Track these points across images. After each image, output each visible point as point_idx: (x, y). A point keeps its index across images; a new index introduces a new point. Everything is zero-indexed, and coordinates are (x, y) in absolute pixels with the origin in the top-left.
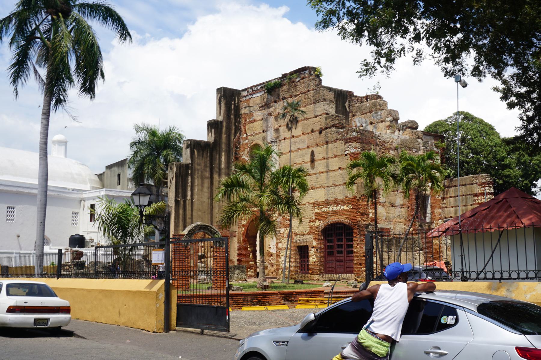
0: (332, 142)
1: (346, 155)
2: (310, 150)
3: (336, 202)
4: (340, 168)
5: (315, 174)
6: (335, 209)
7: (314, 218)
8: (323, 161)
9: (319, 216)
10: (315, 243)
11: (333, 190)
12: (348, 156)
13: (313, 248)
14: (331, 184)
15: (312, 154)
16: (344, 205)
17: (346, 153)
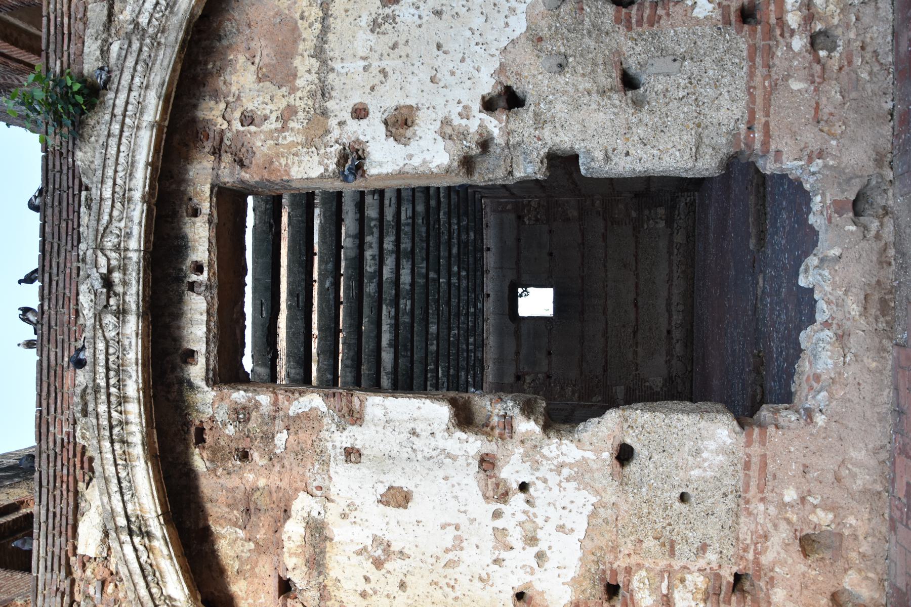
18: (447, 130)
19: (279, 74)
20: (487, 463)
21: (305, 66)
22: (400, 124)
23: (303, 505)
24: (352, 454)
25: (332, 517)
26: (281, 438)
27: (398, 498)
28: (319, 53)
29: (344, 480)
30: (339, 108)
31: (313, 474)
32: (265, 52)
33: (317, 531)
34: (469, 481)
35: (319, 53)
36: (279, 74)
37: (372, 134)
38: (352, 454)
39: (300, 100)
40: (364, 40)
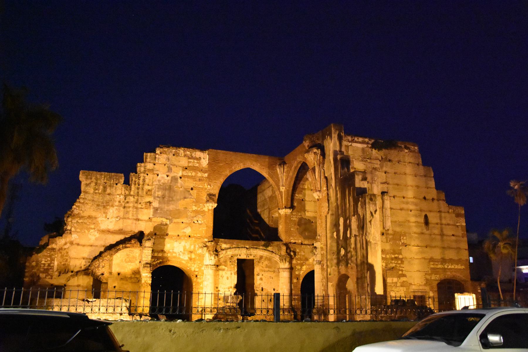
0: (445, 212)
1: (457, 226)
2: (424, 214)
3: (451, 261)
4: (453, 235)
5: (430, 235)
6: (450, 267)
7: (430, 272)
8: (436, 226)
9: (434, 271)
10: (431, 294)
11: (447, 252)
12: (460, 228)
13: (429, 298)
14: (446, 246)
15: (426, 217)
16: (457, 264)
17: (458, 224)
18: (260, 284)
19: (267, 266)
20: (231, 287)
21: (267, 269)
22: (261, 279)
23: (226, 268)
24: (231, 274)
25: (225, 271)
26: (232, 266)
27: (228, 278)
28: (268, 271)
29: (229, 273)
30: (263, 273)
31: (229, 269)
32: (269, 265)
33: (224, 270)
34: (229, 285)
35: (268, 271)
36: (267, 266)
37: (260, 276)
38: (231, 274)
39: (264, 269)
40: (269, 275)
